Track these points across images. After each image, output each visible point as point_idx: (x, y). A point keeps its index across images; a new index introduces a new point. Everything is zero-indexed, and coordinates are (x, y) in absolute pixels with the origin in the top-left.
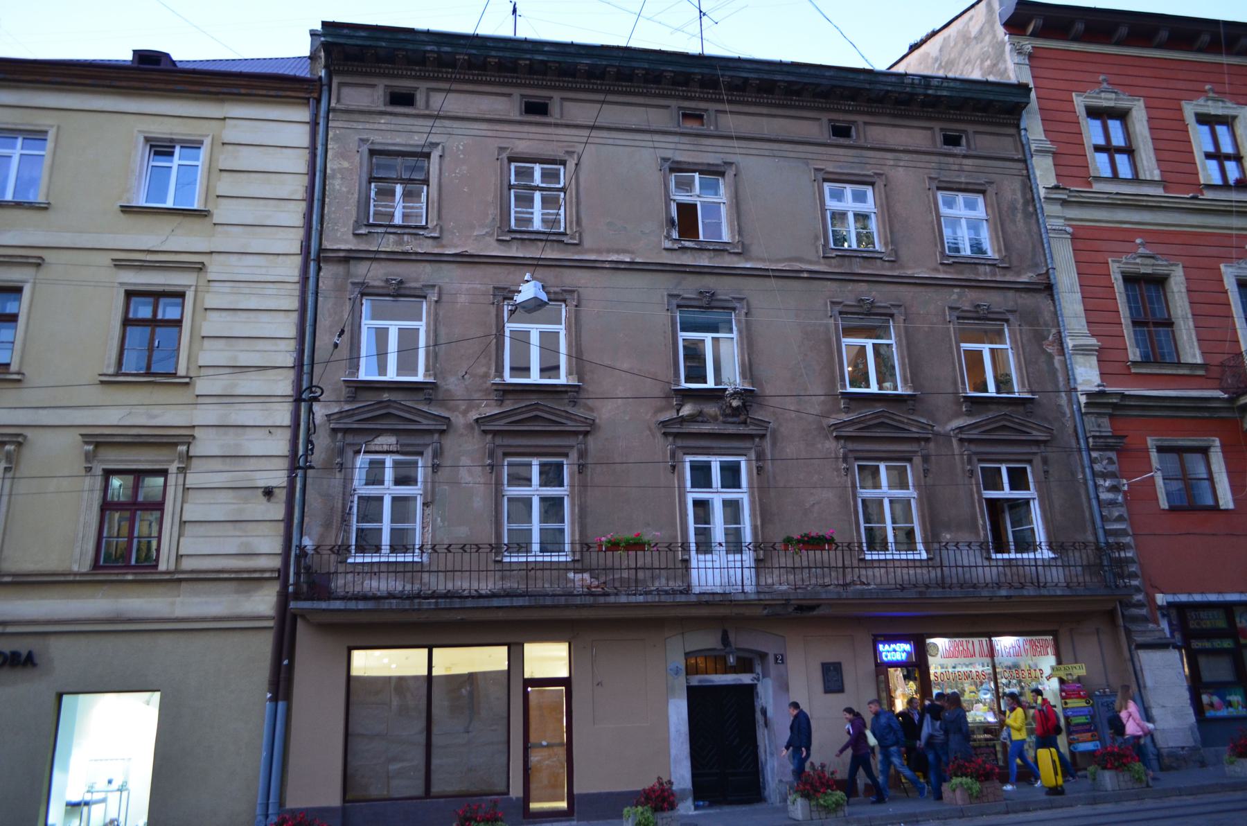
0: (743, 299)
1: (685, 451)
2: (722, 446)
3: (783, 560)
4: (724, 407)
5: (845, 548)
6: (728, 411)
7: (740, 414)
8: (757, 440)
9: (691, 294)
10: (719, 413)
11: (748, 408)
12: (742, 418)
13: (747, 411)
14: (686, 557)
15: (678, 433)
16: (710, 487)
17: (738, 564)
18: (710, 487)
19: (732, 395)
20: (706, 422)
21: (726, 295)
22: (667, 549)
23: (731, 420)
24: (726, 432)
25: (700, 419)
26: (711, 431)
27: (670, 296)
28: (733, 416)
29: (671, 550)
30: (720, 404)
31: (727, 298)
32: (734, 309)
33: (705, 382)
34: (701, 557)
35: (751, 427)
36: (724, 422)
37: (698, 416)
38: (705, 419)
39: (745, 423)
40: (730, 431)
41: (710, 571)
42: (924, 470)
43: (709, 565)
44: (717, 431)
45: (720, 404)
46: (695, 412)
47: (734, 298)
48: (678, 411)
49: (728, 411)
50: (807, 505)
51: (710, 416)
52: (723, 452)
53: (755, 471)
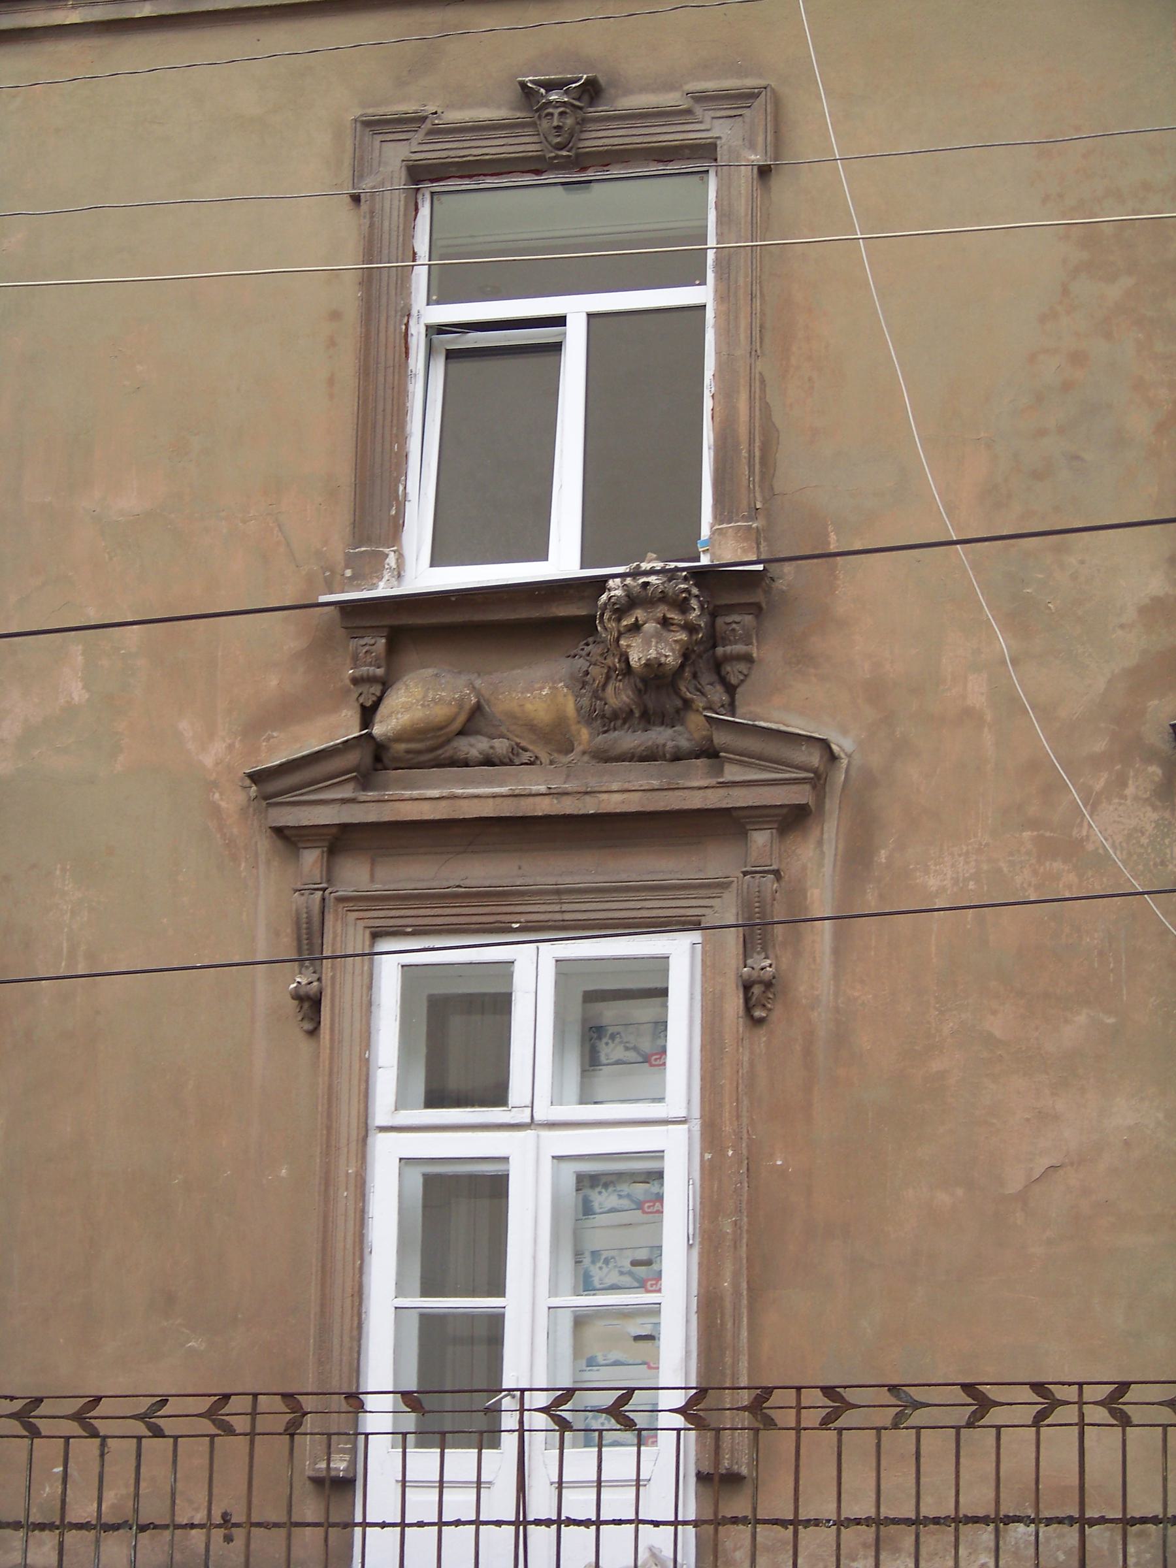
0: (748, 97)
1: (380, 917)
2: (568, 881)
3: (859, 1478)
4: (598, 673)
5: (1099, 1414)
6: (619, 696)
7: (687, 704)
8: (760, 839)
9: (484, 104)
10: (570, 708)
11: (733, 672)
12: (694, 728)
13: (731, 690)
14: (340, 1465)
15: (345, 828)
16: (497, 1095)
17: (500, 1504)
18: (497, 1095)
19: (621, 609)
20: (506, 762)
21: (670, 87)
22: (140, 1428)
23: (630, 739)
24: (589, 806)
25: (474, 747)
26: (507, 809)
27: (374, 125)
28: (648, 718)
29: (158, 1433)
30: (581, 663)
31: (671, 99)
32: (707, 151)
33: (541, 553)
34: (424, 1462)
35: (732, 773)
36: (604, 757)
37: (461, 733)
38: (501, 746)
39: (710, 753)
40: (614, 803)
41: (458, 1540)
42: (747, 987)
43: (459, 1504)
44: (545, 807)
45: (581, 663)
46: (440, 713)
47: (701, 98)
48: (368, 714)
49: (619, 696)
50: (1015, 1182)
51: (531, 727)
52: (575, 909)
53: (734, 1003)
